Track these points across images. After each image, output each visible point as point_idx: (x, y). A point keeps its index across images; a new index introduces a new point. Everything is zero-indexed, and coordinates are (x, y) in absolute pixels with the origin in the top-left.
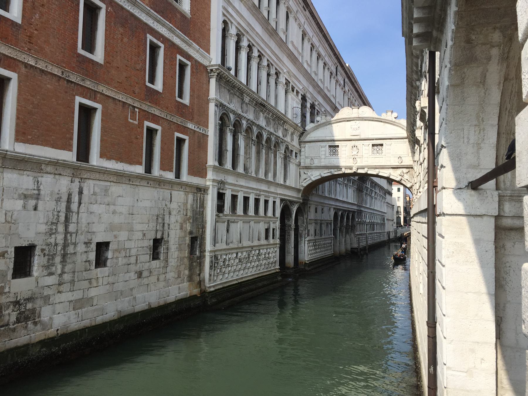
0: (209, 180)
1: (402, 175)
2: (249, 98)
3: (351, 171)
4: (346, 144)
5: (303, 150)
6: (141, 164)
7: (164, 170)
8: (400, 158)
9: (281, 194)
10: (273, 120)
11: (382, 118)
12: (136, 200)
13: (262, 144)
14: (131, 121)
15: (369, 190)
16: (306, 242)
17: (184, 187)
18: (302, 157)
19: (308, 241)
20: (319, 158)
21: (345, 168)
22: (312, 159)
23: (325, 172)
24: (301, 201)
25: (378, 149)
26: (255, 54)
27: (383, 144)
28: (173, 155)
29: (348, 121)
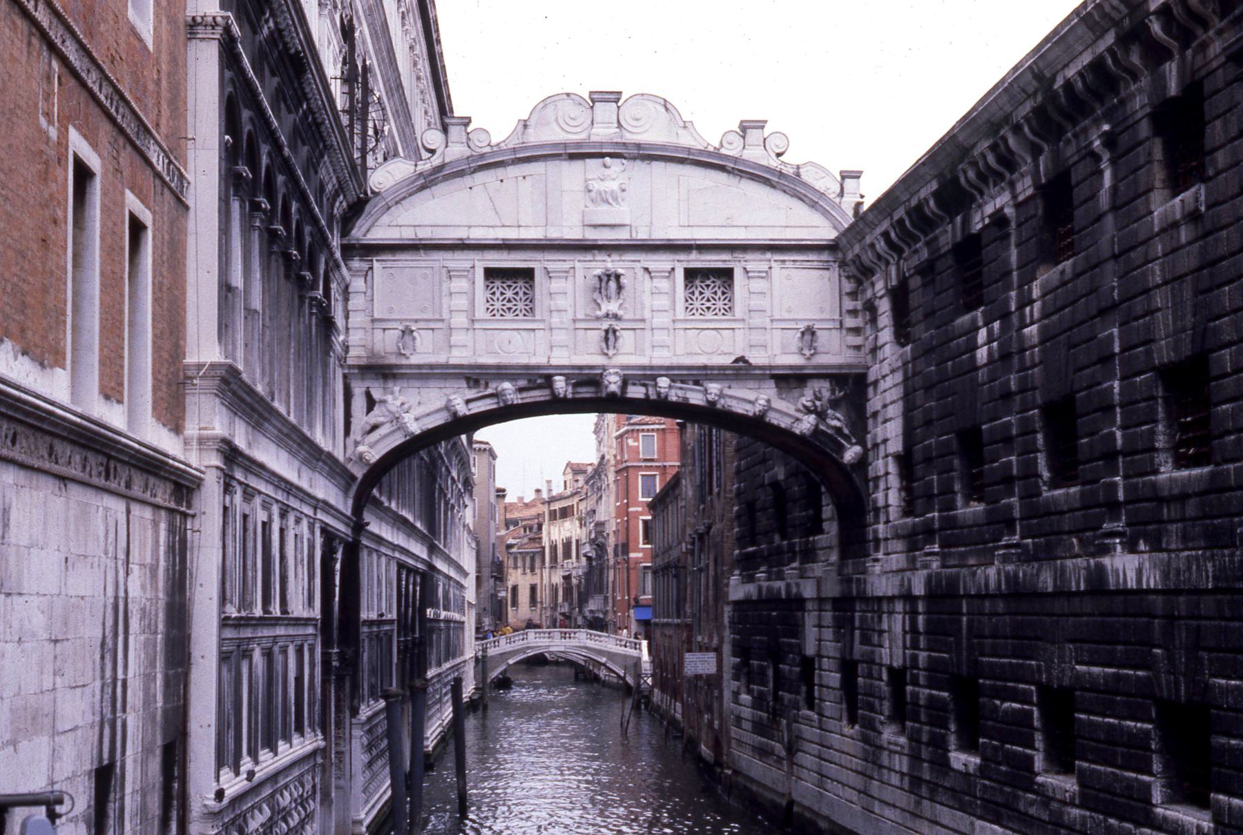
0: (201, 441)
1: (819, 409)
2: (271, 24)
3: (591, 389)
4: (566, 266)
5: (358, 284)
6: (59, 361)
7: (107, 397)
8: (808, 337)
9: (326, 506)
11: (723, 151)
12: (63, 560)
13: (287, 257)
14: (43, 121)
15: (444, 469)
16: (357, 732)
17: (152, 480)
18: (355, 320)
19: (363, 724)
21: (566, 380)
22: (407, 332)
23: (472, 394)
24: (349, 532)
25: (708, 293)
28: (121, 312)
29: (573, 157)
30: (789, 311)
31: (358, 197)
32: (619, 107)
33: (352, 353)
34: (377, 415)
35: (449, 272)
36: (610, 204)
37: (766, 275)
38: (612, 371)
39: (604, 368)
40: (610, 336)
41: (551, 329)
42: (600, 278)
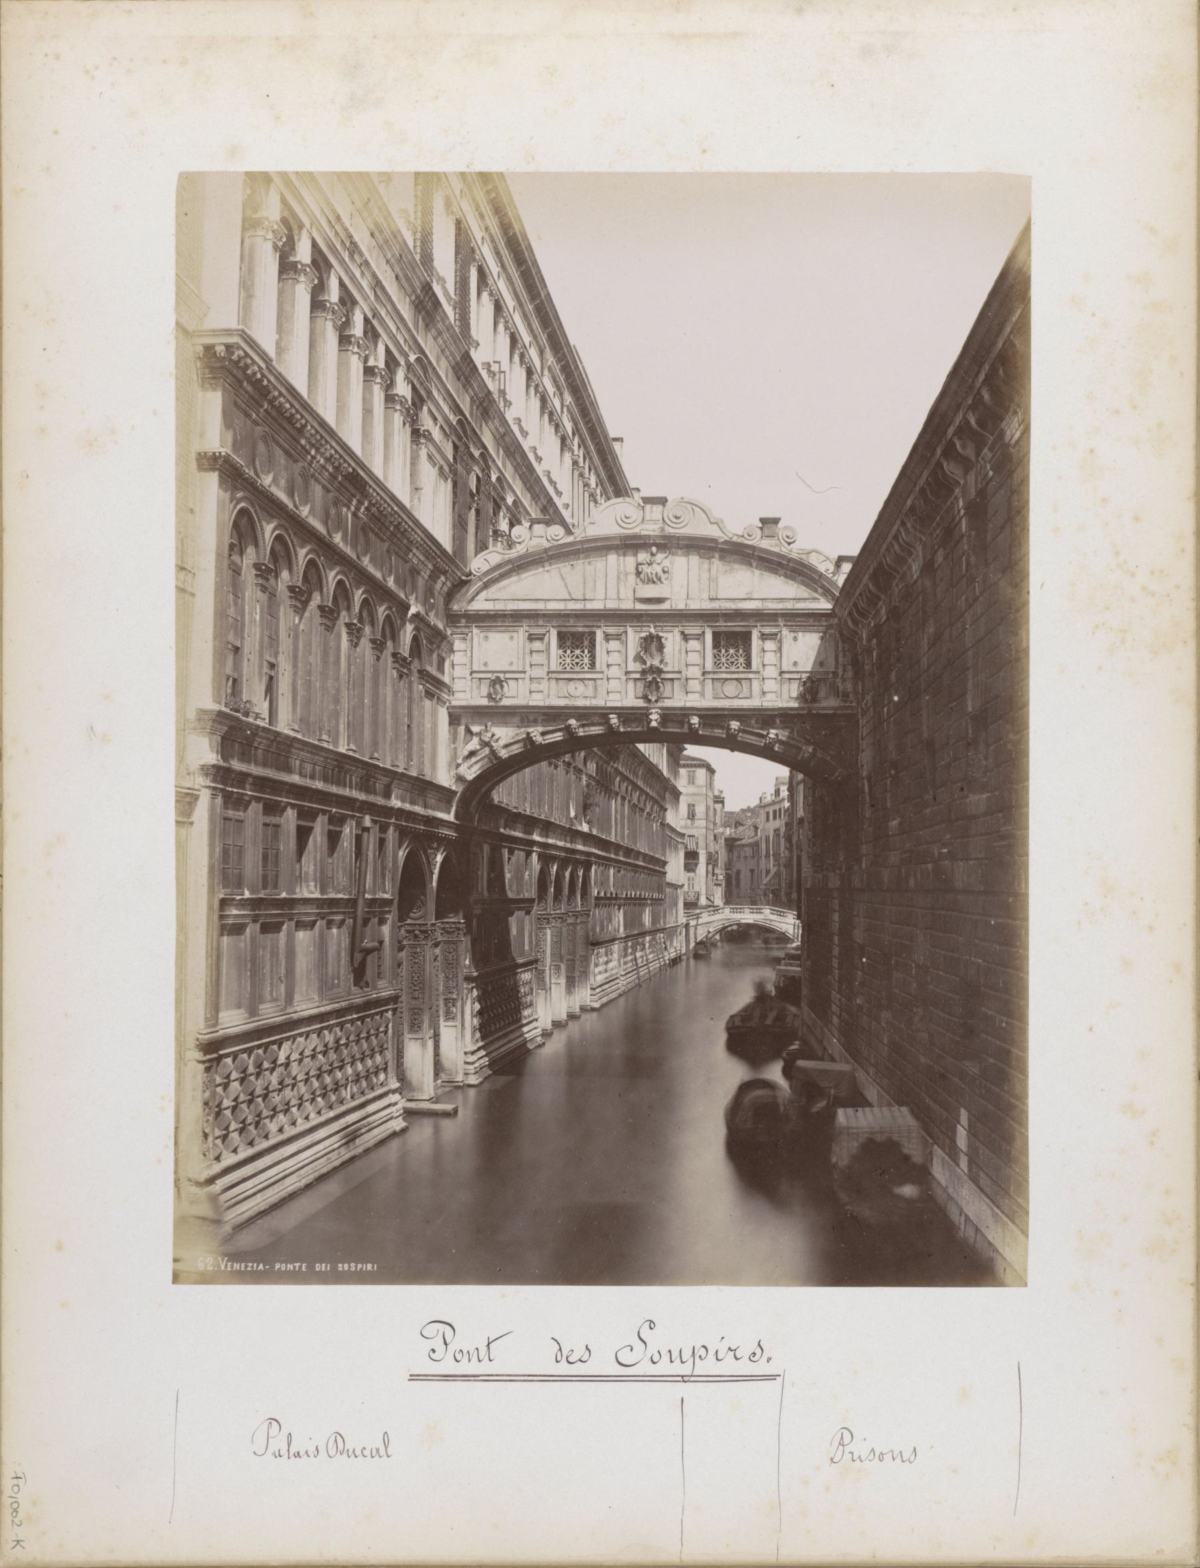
10: (376, 535)
18: (458, 672)
20: (522, 675)
21: (619, 718)
25: (732, 651)
26: (333, 295)
27: (750, 633)
30: (795, 664)
31: (460, 578)
32: (664, 506)
33: (457, 695)
34: (474, 744)
35: (530, 635)
36: (654, 582)
37: (773, 636)
38: (653, 711)
39: (647, 709)
40: (653, 686)
41: (608, 679)
42: (645, 639)
